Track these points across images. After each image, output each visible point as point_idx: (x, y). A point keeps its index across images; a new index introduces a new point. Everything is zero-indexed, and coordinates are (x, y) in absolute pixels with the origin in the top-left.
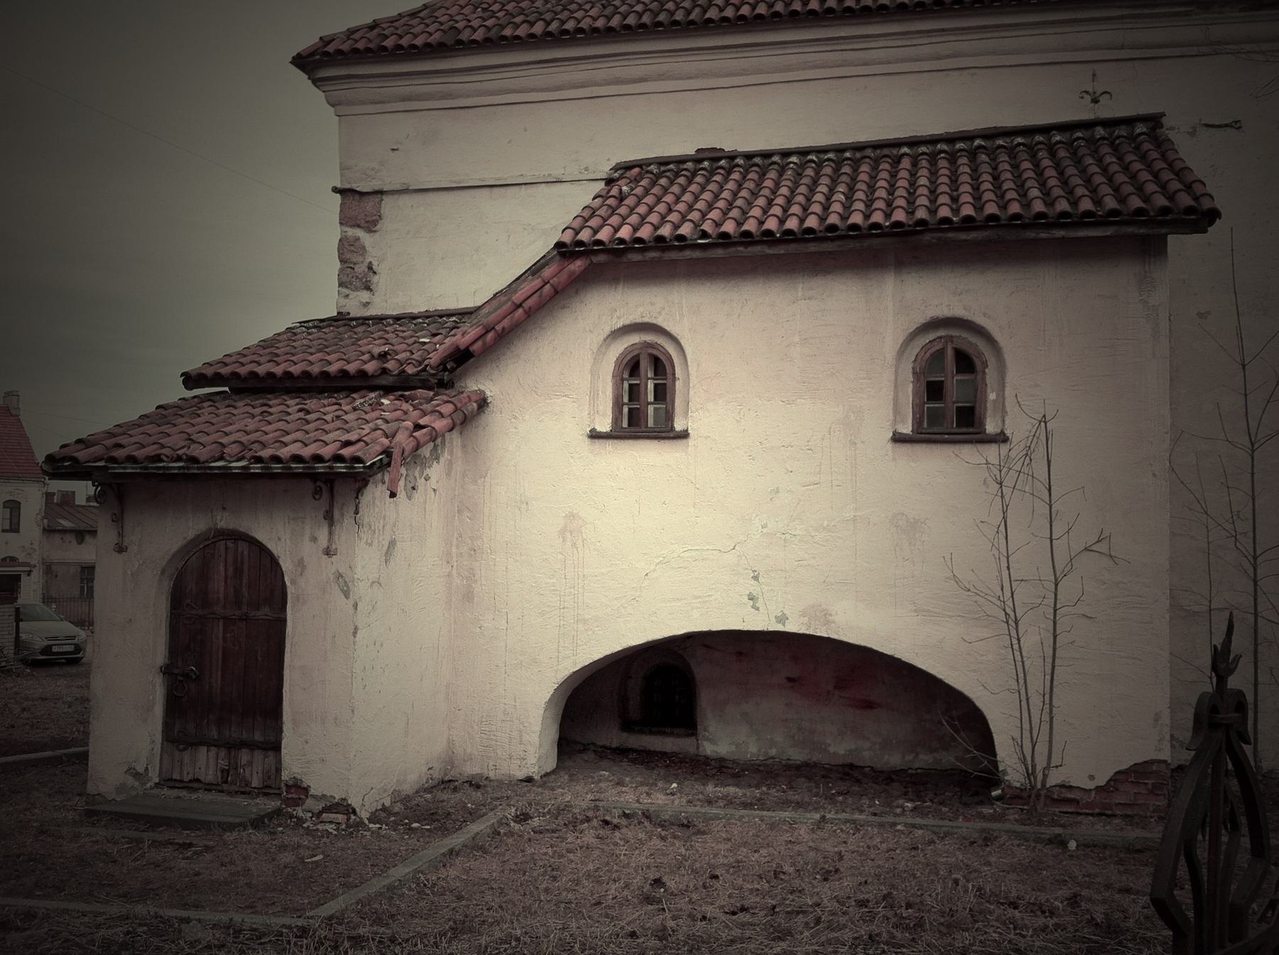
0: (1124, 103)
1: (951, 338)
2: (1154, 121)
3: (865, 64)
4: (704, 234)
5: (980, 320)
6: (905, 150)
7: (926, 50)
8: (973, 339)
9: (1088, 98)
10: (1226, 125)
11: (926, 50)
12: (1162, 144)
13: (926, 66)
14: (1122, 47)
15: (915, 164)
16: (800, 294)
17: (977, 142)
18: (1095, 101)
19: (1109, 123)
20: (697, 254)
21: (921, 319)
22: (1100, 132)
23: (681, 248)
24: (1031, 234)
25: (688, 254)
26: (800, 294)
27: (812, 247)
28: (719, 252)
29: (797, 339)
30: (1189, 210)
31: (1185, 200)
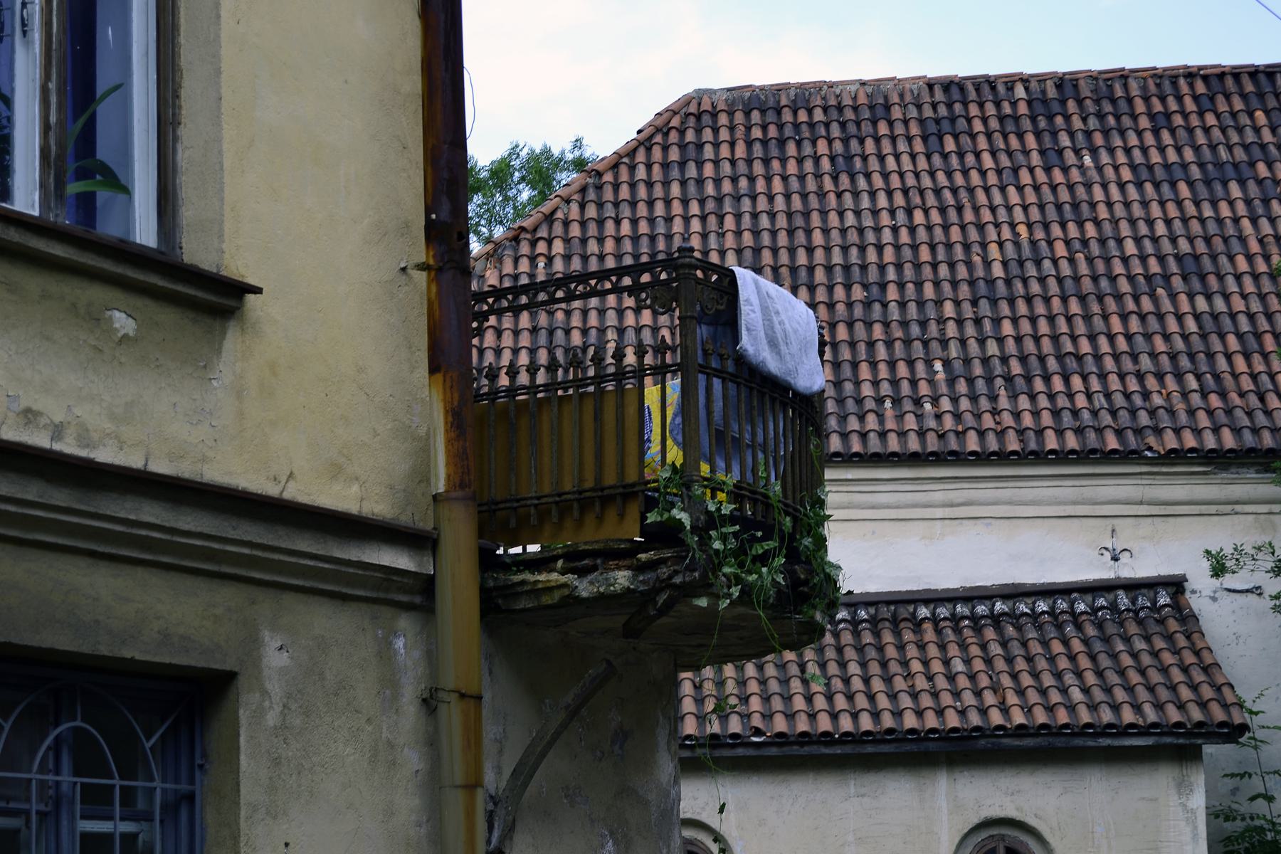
0: (1145, 564)
1: (1002, 837)
2: (1176, 585)
3: (873, 508)
4: (758, 732)
5: (1032, 821)
6: (923, 612)
7: (938, 497)
8: (1024, 837)
9: (1108, 555)
10: (1247, 591)
11: (938, 497)
12: (1188, 619)
13: (939, 513)
14: (1141, 503)
15: (938, 631)
16: (852, 790)
17: (999, 606)
18: (1115, 559)
19: (1133, 587)
20: (751, 752)
21: (975, 820)
22: (1123, 600)
23: (733, 746)
24: (1079, 742)
25: (740, 751)
26: (852, 790)
27: (870, 749)
28: (773, 751)
29: (851, 838)
30: (1222, 724)
31: (1219, 715)
